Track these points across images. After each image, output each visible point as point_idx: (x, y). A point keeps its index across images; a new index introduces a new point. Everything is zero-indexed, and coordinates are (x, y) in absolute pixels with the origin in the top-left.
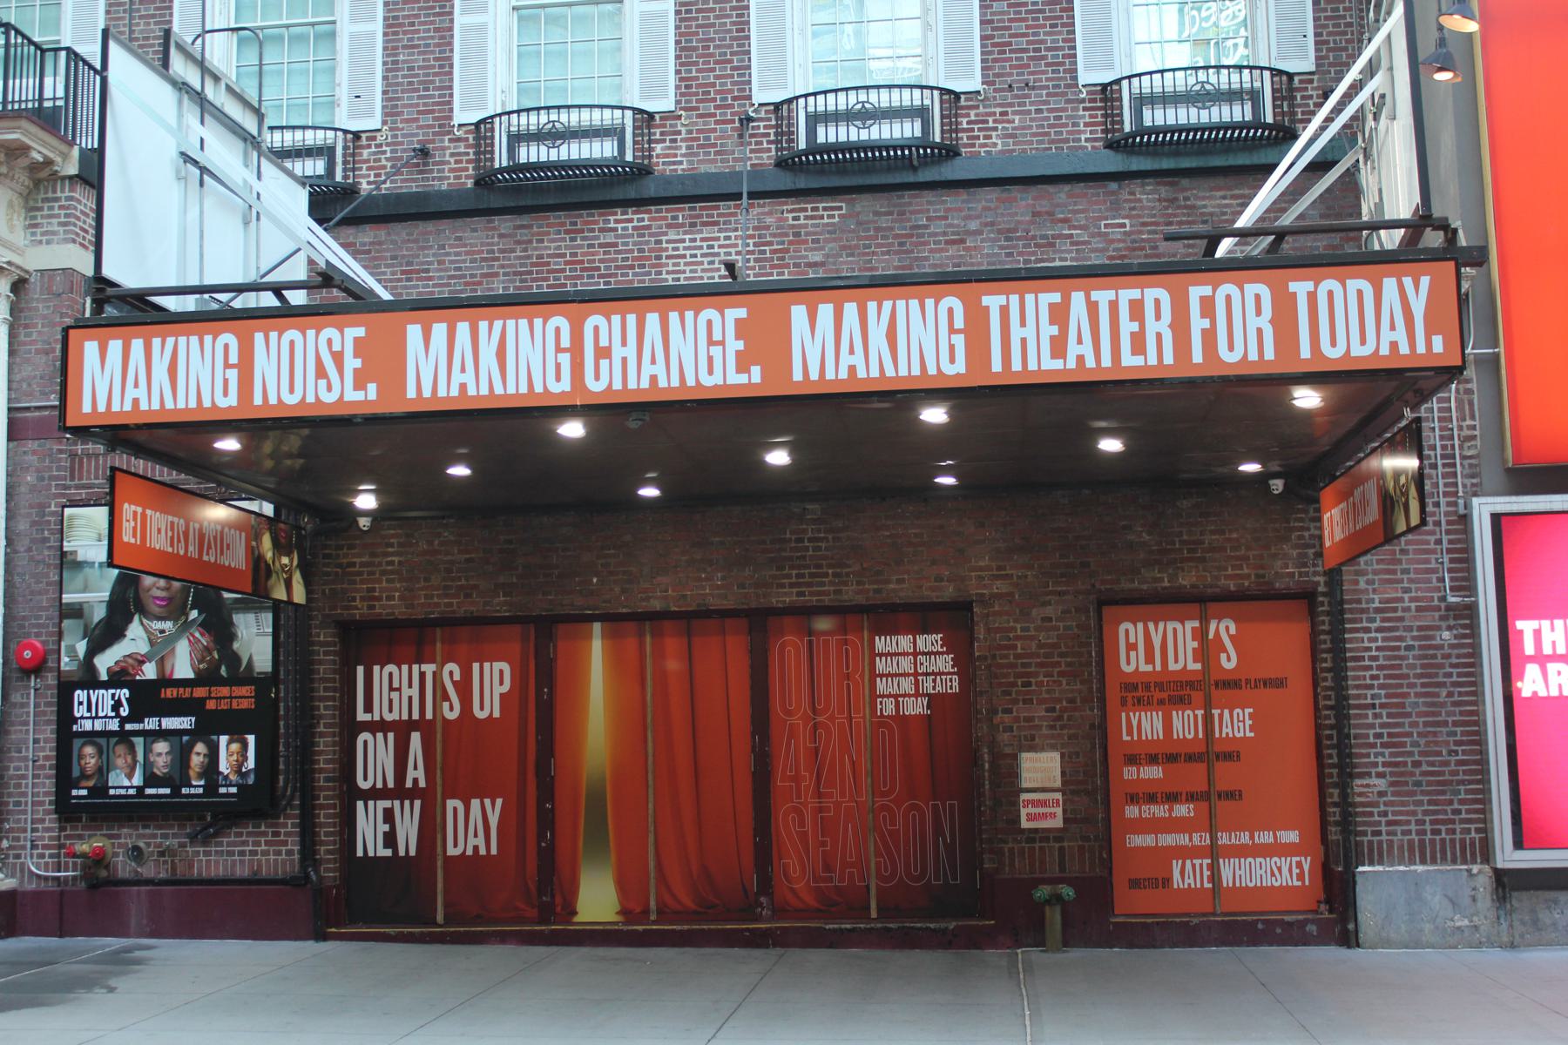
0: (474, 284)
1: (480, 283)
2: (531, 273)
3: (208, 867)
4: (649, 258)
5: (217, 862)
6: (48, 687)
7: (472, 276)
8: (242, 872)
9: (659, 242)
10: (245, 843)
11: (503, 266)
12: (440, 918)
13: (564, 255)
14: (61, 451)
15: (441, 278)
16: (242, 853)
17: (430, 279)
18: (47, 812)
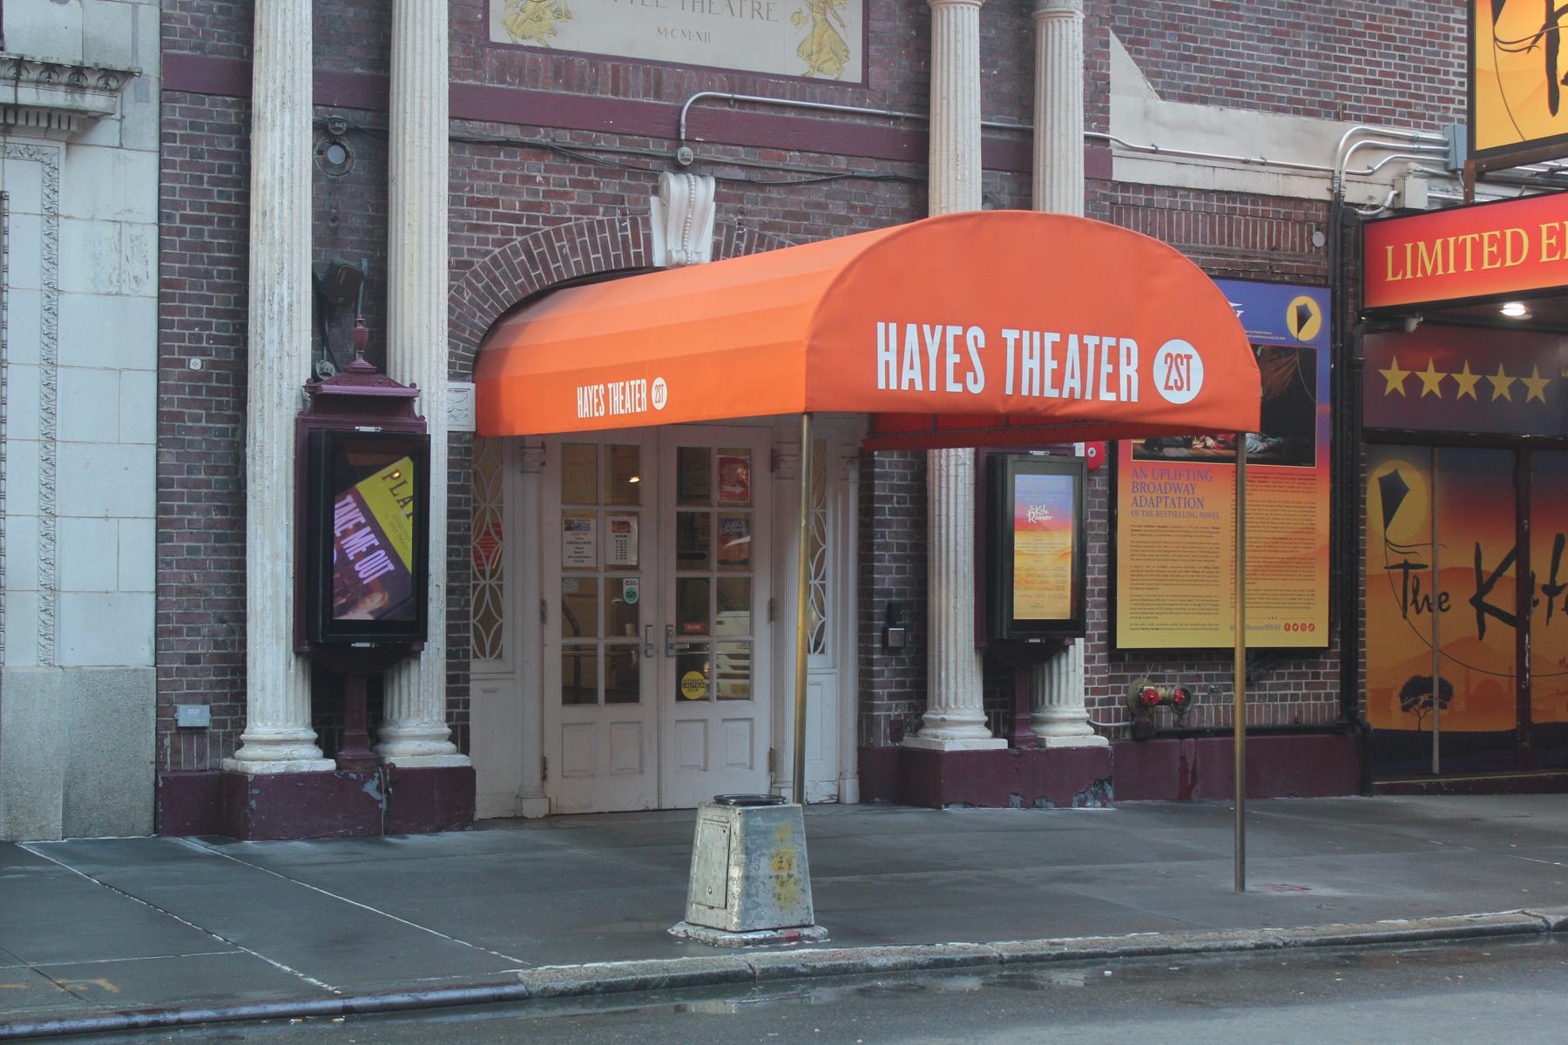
0: (1282, 33)
1: (1287, 34)
2: (1333, 31)
3: (1275, 712)
4: (1437, 36)
5: (1259, 708)
6: (1096, 493)
7: (1280, 23)
8: (1284, 719)
9: (1447, 19)
10: (1287, 686)
11: (1308, 18)
12: (1436, 769)
13: (1363, 17)
14: (1105, 197)
15: (1250, 19)
16: (1284, 698)
17: (1239, 18)
18: (1096, 649)
